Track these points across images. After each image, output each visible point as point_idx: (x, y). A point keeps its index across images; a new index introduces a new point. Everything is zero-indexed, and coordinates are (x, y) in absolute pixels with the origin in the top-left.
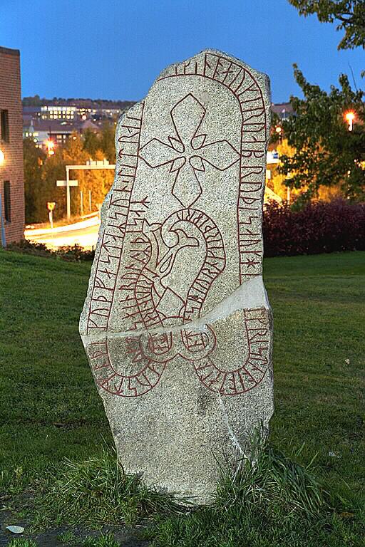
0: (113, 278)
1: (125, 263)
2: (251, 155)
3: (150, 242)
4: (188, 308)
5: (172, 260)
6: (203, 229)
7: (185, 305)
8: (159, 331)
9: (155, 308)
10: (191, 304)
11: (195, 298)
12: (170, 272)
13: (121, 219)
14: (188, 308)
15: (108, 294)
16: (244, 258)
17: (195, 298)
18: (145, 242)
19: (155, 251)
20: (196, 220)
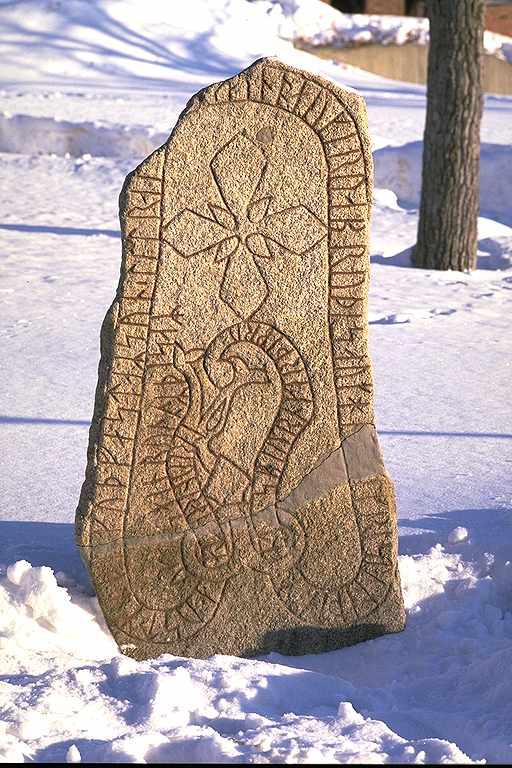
0: (129, 445)
1: (149, 418)
2: (344, 227)
3: (188, 380)
4: (259, 487)
5: (227, 407)
6: (274, 352)
7: (253, 483)
8: (209, 531)
9: (204, 491)
10: (264, 479)
11: (269, 470)
12: (223, 430)
13: (139, 347)
14: (259, 487)
15: (124, 475)
16: (345, 396)
17: (269, 470)
18: (179, 382)
19: (197, 396)
20: (261, 341)
